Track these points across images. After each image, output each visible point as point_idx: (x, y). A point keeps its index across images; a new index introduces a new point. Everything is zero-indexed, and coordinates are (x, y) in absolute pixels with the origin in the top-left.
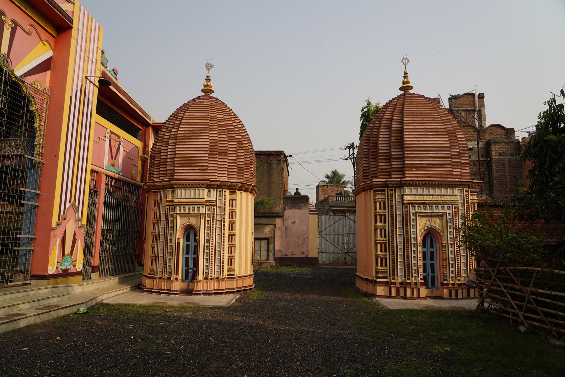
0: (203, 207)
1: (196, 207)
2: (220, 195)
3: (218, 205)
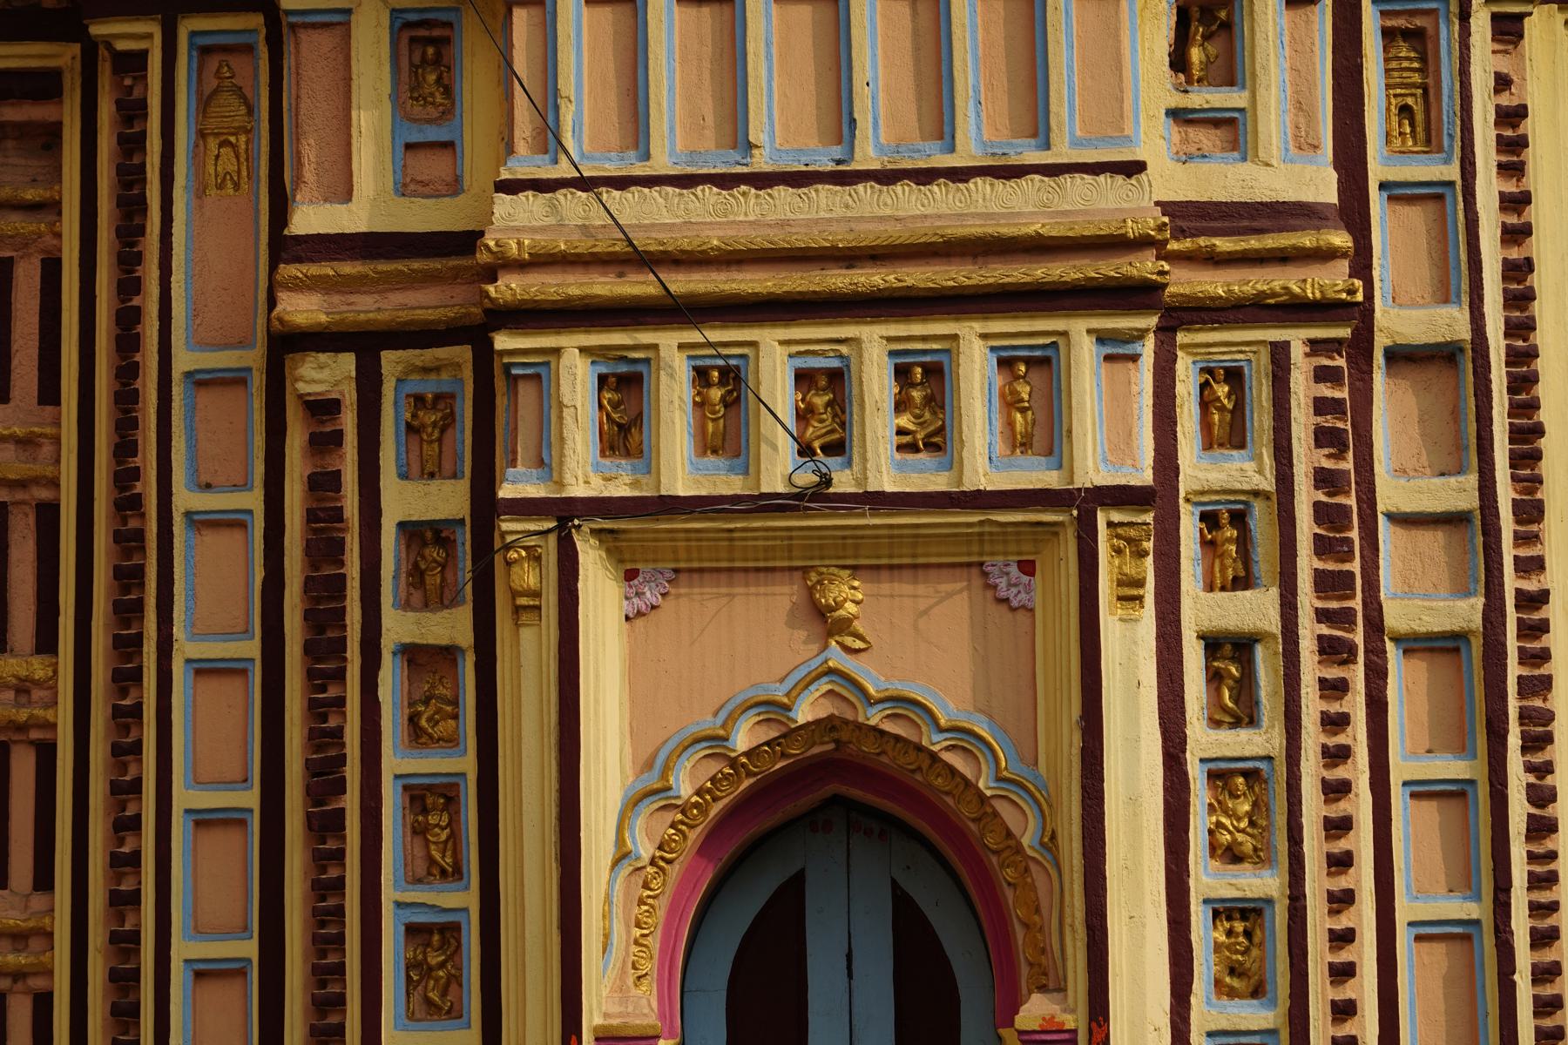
0: (1118, 352)
1: (974, 352)
2: (1421, 122)
3: (1402, 319)
